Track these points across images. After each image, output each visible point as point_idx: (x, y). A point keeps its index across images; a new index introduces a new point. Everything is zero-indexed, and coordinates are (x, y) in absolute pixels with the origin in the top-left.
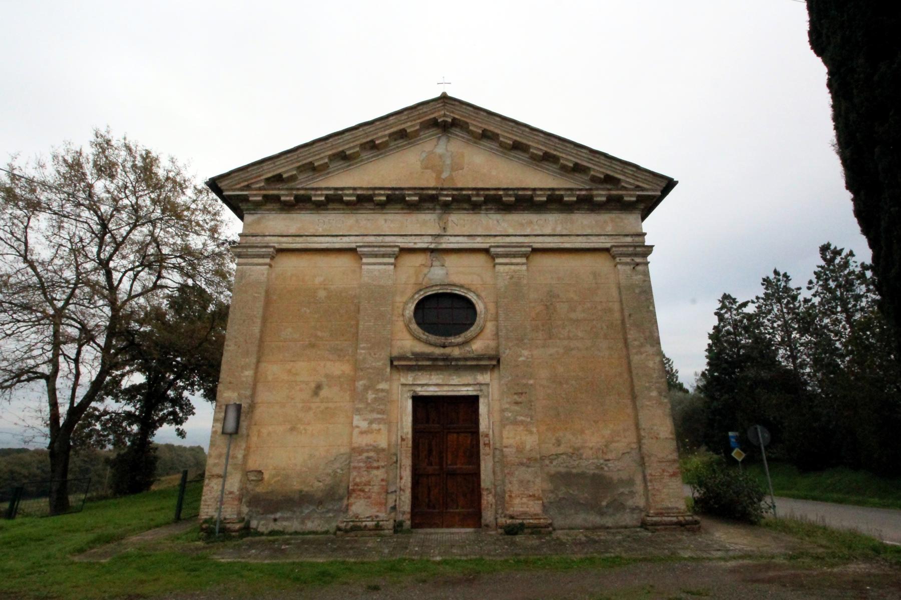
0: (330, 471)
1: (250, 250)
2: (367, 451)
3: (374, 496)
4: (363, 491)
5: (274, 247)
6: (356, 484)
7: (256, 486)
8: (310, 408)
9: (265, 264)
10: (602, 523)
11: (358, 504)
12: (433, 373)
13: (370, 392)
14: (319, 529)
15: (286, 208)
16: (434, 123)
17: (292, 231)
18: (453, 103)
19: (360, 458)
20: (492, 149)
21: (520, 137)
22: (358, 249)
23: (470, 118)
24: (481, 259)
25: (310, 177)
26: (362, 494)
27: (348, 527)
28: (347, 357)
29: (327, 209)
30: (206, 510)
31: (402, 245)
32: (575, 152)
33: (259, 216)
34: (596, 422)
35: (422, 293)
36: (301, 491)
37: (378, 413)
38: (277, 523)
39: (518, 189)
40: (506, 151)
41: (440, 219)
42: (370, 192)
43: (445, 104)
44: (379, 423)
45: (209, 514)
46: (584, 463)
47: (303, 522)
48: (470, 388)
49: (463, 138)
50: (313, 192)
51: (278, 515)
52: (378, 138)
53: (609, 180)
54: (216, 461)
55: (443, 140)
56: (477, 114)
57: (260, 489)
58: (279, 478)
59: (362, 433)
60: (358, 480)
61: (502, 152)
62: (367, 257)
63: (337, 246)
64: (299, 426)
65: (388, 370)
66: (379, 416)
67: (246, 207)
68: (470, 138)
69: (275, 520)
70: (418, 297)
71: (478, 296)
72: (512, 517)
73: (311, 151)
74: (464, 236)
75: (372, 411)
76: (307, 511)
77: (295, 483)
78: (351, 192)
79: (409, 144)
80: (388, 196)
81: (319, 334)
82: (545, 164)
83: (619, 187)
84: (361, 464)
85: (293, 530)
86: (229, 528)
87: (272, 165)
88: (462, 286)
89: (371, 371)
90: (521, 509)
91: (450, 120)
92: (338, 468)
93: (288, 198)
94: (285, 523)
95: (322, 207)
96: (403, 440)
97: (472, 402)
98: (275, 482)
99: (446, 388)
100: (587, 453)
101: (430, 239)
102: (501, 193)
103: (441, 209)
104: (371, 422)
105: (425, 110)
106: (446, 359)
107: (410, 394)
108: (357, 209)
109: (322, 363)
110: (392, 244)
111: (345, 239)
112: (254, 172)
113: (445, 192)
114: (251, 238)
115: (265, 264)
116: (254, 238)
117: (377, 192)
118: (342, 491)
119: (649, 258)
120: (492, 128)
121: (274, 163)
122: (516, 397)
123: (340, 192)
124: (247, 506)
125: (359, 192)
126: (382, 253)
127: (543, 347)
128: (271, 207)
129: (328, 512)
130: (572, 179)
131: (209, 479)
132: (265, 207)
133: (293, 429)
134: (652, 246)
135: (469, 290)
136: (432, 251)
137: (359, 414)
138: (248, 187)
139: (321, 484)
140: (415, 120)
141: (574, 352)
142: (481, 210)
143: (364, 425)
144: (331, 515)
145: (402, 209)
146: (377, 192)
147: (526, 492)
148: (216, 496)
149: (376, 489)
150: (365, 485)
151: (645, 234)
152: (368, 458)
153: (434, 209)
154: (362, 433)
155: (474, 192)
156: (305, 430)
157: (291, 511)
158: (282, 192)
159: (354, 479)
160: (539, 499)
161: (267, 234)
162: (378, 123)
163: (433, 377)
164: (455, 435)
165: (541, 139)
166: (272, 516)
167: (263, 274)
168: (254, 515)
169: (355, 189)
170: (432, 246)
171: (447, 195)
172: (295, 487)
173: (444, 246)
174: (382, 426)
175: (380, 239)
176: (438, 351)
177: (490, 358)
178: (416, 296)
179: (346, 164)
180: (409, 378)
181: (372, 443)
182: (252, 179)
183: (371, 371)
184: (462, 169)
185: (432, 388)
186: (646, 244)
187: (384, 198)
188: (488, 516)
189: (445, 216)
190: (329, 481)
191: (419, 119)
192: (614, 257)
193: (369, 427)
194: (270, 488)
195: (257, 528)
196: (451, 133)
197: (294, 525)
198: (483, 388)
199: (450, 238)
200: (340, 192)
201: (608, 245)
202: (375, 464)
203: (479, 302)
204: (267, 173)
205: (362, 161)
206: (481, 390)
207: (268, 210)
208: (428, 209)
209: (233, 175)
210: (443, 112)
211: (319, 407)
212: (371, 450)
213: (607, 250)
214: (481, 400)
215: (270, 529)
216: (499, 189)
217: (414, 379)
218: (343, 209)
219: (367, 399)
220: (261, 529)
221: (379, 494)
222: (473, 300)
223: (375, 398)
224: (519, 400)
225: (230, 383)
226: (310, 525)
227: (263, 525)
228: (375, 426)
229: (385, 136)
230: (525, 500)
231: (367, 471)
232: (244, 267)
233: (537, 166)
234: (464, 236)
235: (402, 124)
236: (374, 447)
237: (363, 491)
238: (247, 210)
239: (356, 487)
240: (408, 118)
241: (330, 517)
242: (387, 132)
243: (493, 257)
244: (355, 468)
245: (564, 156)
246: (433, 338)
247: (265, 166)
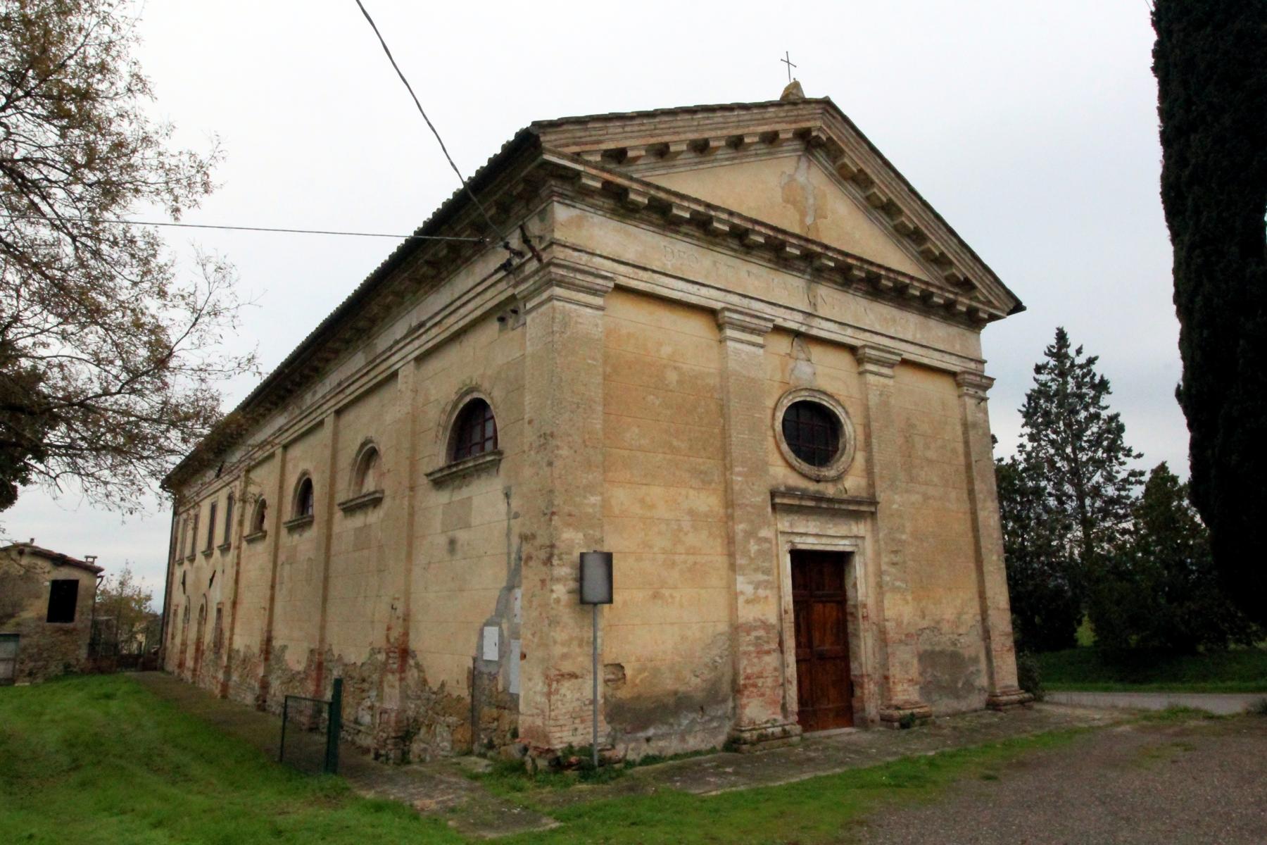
0: (707, 660)
1: (579, 276)
2: (755, 628)
3: (768, 692)
4: (755, 686)
6: (748, 678)
7: (618, 688)
8: (674, 564)
10: (959, 707)
11: (751, 705)
12: (809, 518)
13: (752, 542)
14: (703, 747)
15: (622, 211)
16: (803, 136)
17: (629, 256)
18: (835, 115)
19: (748, 639)
20: (855, 198)
21: (896, 196)
23: (847, 145)
24: (844, 360)
25: (651, 166)
26: (755, 690)
27: (755, 737)
28: (713, 485)
29: (677, 232)
30: (559, 735)
32: (946, 238)
33: (577, 212)
34: (950, 589)
36: (676, 693)
37: (763, 573)
38: (651, 743)
40: (870, 207)
41: (809, 288)
42: (749, 226)
44: (766, 588)
45: (565, 740)
46: (944, 639)
47: (683, 739)
48: (846, 542)
49: (826, 168)
50: (678, 201)
51: (651, 732)
53: (966, 286)
54: (565, 650)
55: (804, 164)
56: (858, 143)
57: (624, 693)
58: (646, 674)
59: (748, 602)
60: (749, 671)
61: (865, 207)
62: (733, 329)
63: (694, 300)
64: (663, 591)
65: (769, 509)
66: (765, 578)
67: (561, 191)
68: (834, 172)
69: (648, 740)
71: (847, 413)
72: (898, 708)
73: (672, 125)
74: (835, 322)
75: (756, 570)
76: (685, 722)
77: (668, 681)
78: (724, 216)
79: (769, 153)
80: (767, 237)
81: (675, 443)
82: (906, 242)
83: (972, 295)
84: (751, 648)
85: (670, 752)
86: (610, 758)
87: (620, 130)
88: (831, 396)
89: (749, 509)
90: (905, 698)
91: (824, 138)
92: (717, 655)
93: (640, 199)
94: (661, 744)
95: (672, 227)
97: (798, 557)
98: (642, 681)
99: (824, 540)
100: (945, 627)
101: (799, 317)
102: (883, 272)
103: (811, 275)
104: (757, 586)
105: (805, 112)
106: (819, 498)
107: (787, 547)
108: (716, 244)
109: (684, 492)
110: (759, 314)
111: (704, 291)
112: (595, 130)
113: (830, 254)
114: (570, 251)
116: (576, 254)
117: (757, 228)
118: (726, 687)
119: (989, 393)
120: (868, 171)
121: (623, 127)
123: (713, 213)
124: (609, 723)
125: (736, 221)
126: (753, 326)
127: (907, 491)
128: (601, 203)
129: (712, 720)
130: (928, 270)
131: (558, 681)
132: (591, 201)
133: (656, 596)
134: (992, 380)
135: (838, 402)
136: (797, 334)
137: (743, 575)
138: (576, 157)
139: (698, 680)
141: (931, 501)
143: (749, 590)
144: (715, 724)
145: (770, 261)
146: (757, 228)
147: (906, 676)
148: (571, 709)
149: (770, 682)
150: (758, 677)
151: (985, 362)
152: (758, 638)
153: (803, 272)
154: (748, 602)
155: (859, 264)
156: (671, 596)
157: (666, 723)
158: (635, 186)
159: (745, 668)
160: (917, 683)
161: (598, 252)
162: (755, 111)
163: (809, 523)
164: (821, 605)
165: (917, 207)
166: (641, 735)
167: (597, 325)
168: (619, 735)
169: (731, 213)
170: (803, 329)
171: (831, 259)
172: (668, 687)
173: (814, 332)
174: (768, 592)
175: (746, 302)
176: (812, 487)
179: (696, 160)
180: (784, 523)
181: (761, 617)
182: (586, 144)
183: (749, 509)
184: (826, 218)
185: (811, 540)
186: (986, 374)
187: (761, 240)
188: (872, 709)
189: (813, 285)
190: (708, 675)
192: (959, 385)
193: (755, 593)
194: (636, 690)
195: (625, 755)
196: (813, 155)
197: (672, 746)
198: (859, 542)
199: (820, 321)
200: (713, 213)
201: (957, 369)
202: (766, 647)
203: (848, 422)
204: (612, 140)
206: (856, 545)
207: (592, 206)
208: (799, 270)
209: (565, 127)
210: (819, 123)
211: (685, 562)
212: (759, 627)
213: (953, 375)
214: (858, 561)
215: (642, 754)
216: (880, 266)
217: (791, 526)
218: (698, 239)
219: (749, 551)
220: (631, 756)
221: (773, 688)
222: (841, 418)
223: (759, 550)
224: (895, 560)
225: (570, 515)
226: (693, 743)
227: (632, 750)
228: (761, 592)
230: (906, 686)
231: (759, 658)
232: (568, 306)
233: (898, 241)
234: (835, 322)
235: (778, 122)
236: (762, 622)
237: (755, 686)
238: (561, 195)
239: (747, 681)
240: (787, 116)
241: (715, 728)
243: (860, 361)
244: (745, 653)
245: (933, 238)
246: (805, 467)
247: (614, 127)
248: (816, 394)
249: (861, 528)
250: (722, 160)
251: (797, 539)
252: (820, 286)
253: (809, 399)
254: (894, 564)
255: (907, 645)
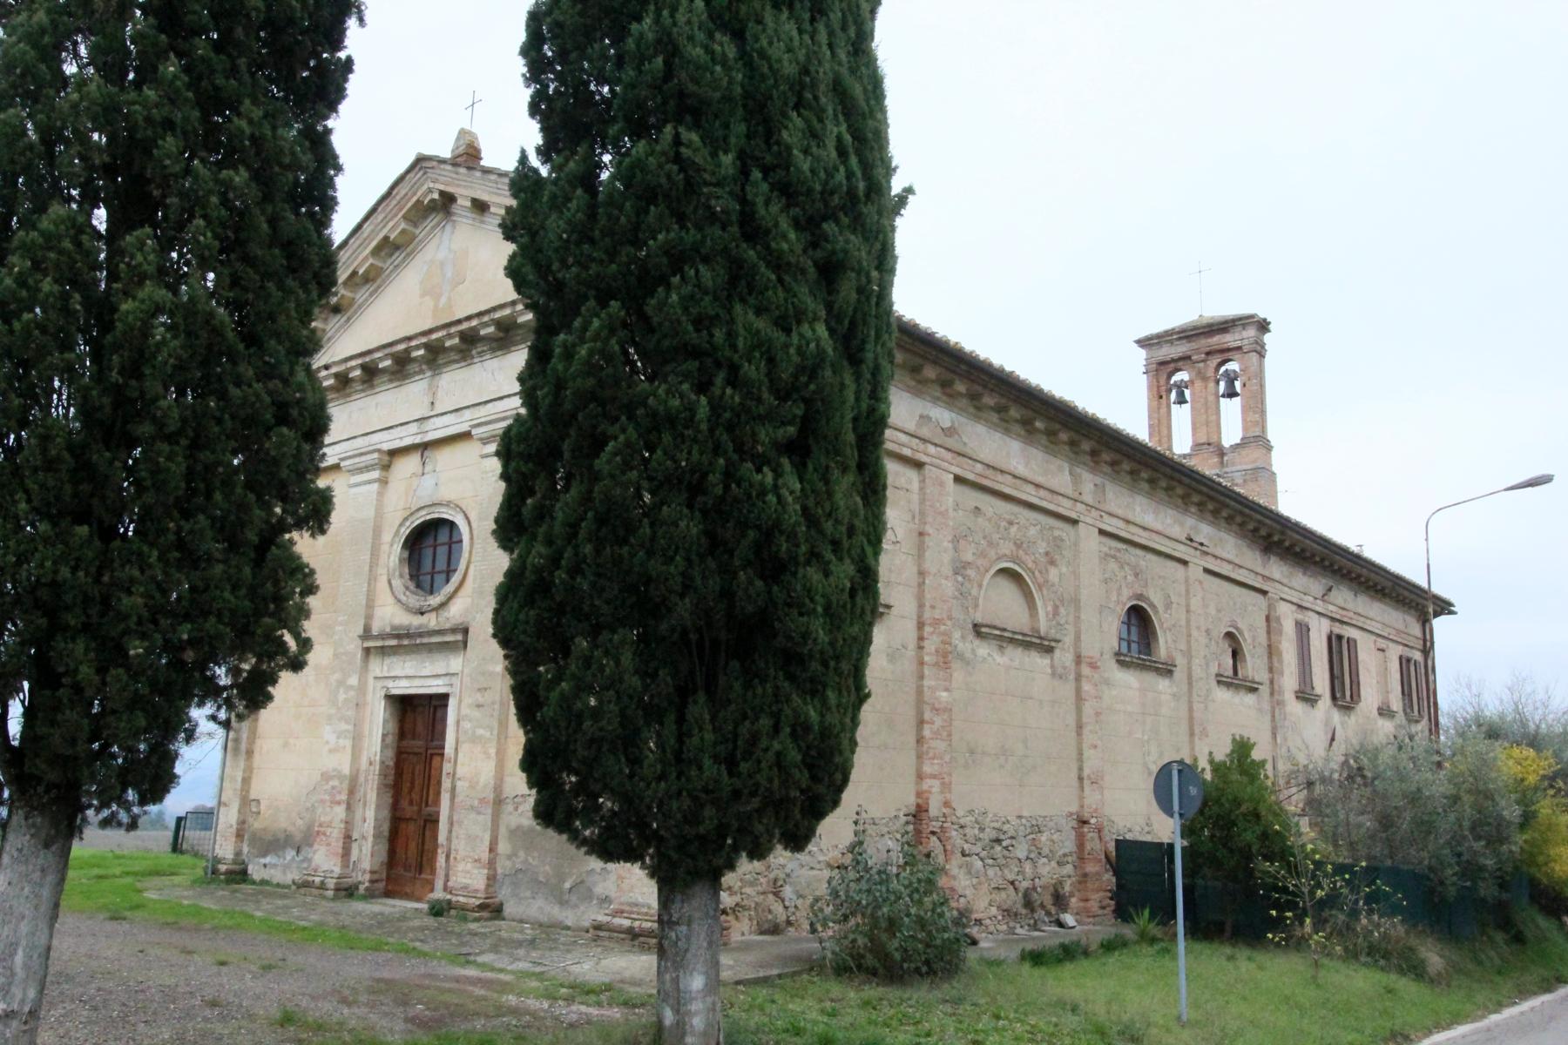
5: (379, 451)
6: (320, 825)
9: (369, 482)
10: (561, 918)
13: (341, 690)
22: (342, 464)
31: (386, 447)
35: (408, 524)
39: (494, 309)
43: (425, 170)
47: (284, 873)
48: (440, 682)
51: (267, 860)
52: (359, 265)
70: (405, 531)
79: (408, 255)
84: (327, 797)
90: (464, 881)
91: (436, 196)
94: (272, 871)
96: (371, 764)
99: (417, 682)
102: (474, 323)
103: (430, 369)
105: (403, 192)
115: (369, 482)
122: (479, 695)
125: (334, 370)
140: (396, 215)
142: (473, 358)
152: (333, 788)
153: (421, 372)
166: (263, 861)
170: (418, 440)
177: (453, 631)
178: (403, 530)
179: (345, 318)
185: (404, 683)
191: (401, 210)
202: (338, 798)
205: (360, 307)
214: (452, 703)
216: (469, 318)
229: (366, 259)
230: (469, 865)
237: (324, 834)
242: (368, 251)
248: (433, 509)
249: (455, 663)
250: (366, 300)
251: (390, 684)
252: (444, 376)
253: (428, 517)
254: (479, 706)
255: (479, 813)
